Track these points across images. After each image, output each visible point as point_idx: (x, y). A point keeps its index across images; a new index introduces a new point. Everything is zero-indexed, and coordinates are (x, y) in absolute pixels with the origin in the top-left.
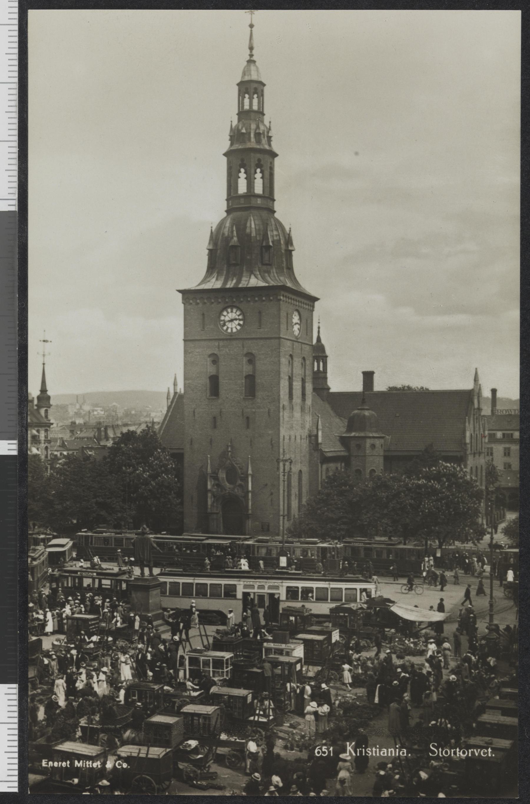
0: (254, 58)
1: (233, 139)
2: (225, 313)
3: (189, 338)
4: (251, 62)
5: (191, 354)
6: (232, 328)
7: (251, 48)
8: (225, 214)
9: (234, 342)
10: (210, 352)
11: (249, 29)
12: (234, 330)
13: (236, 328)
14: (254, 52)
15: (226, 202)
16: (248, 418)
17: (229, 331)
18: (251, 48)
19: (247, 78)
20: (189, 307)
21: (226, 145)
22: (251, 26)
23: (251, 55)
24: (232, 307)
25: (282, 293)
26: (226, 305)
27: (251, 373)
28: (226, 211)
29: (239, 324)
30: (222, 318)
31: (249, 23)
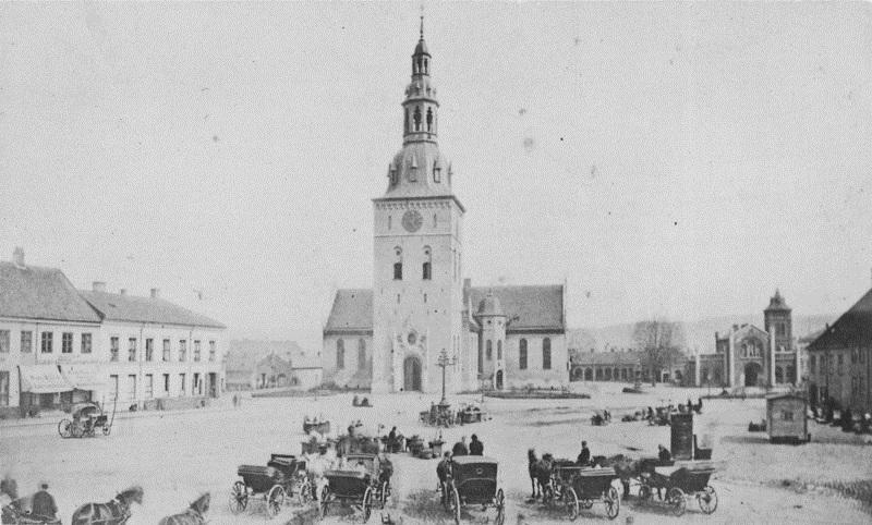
7: (422, 32)
14: (424, 35)
18: (422, 32)
21: (404, 98)
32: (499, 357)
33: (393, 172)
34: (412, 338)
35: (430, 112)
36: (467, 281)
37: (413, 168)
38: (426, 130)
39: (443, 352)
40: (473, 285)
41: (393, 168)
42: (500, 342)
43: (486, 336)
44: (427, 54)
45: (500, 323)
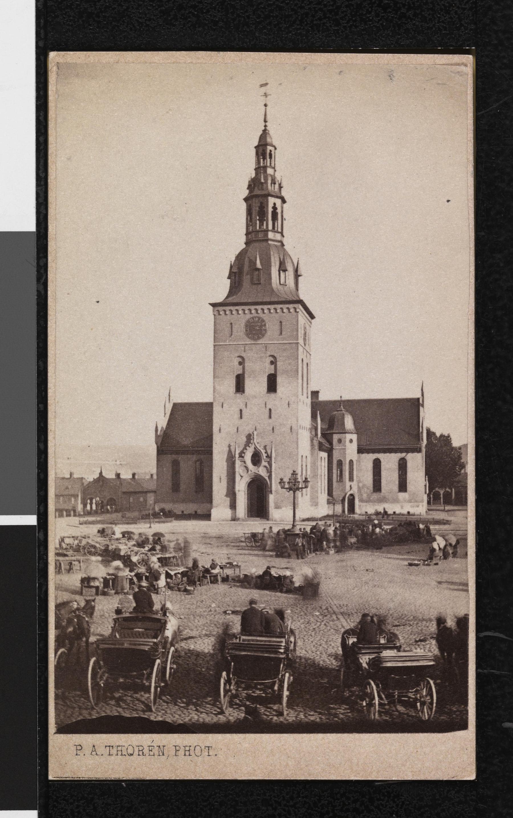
0: (267, 128)
1: (249, 187)
4: (265, 131)
7: (265, 121)
8: (244, 246)
11: (264, 108)
15: (245, 236)
16: (270, 410)
18: (265, 121)
19: (262, 143)
21: (245, 193)
22: (266, 105)
23: (265, 126)
25: (300, 307)
28: (245, 243)
31: (264, 104)
32: (351, 479)
33: (235, 273)
34: (256, 459)
35: (275, 208)
36: (315, 394)
37: (258, 270)
38: (270, 227)
39: (294, 473)
40: (322, 397)
41: (235, 270)
42: (351, 462)
43: (336, 456)
45: (351, 441)
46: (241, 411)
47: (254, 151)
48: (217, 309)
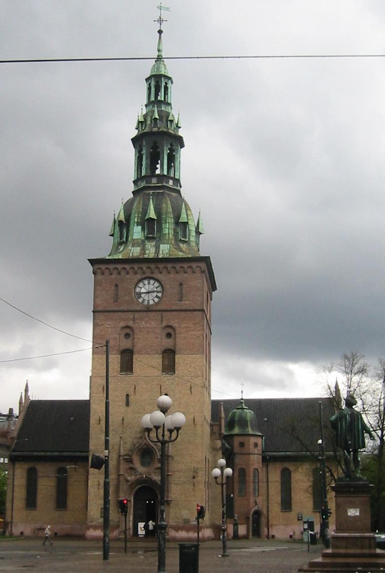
2: (141, 285)
3: (99, 309)
5: (101, 327)
6: (148, 300)
9: (151, 314)
10: (122, 324)
11: (159, 35)
12: (151, 302)
13: (154, 301)
17: (146, 302)
20: (100, 277)
22: (160, 32)
24: (149, 278)
26: (144, 276)
27: (170, 347)
29: (157, 297)
30: (138, 290)
44: (170, 78)
46: (127, 395)
47: (145, 86)
48: (97, 266)
